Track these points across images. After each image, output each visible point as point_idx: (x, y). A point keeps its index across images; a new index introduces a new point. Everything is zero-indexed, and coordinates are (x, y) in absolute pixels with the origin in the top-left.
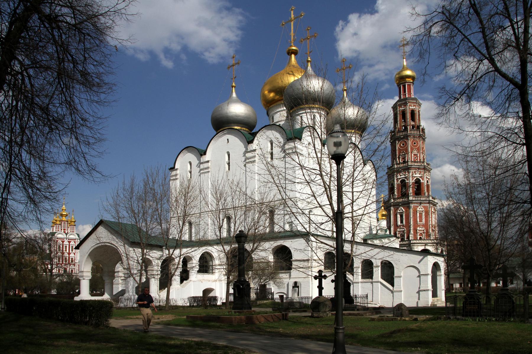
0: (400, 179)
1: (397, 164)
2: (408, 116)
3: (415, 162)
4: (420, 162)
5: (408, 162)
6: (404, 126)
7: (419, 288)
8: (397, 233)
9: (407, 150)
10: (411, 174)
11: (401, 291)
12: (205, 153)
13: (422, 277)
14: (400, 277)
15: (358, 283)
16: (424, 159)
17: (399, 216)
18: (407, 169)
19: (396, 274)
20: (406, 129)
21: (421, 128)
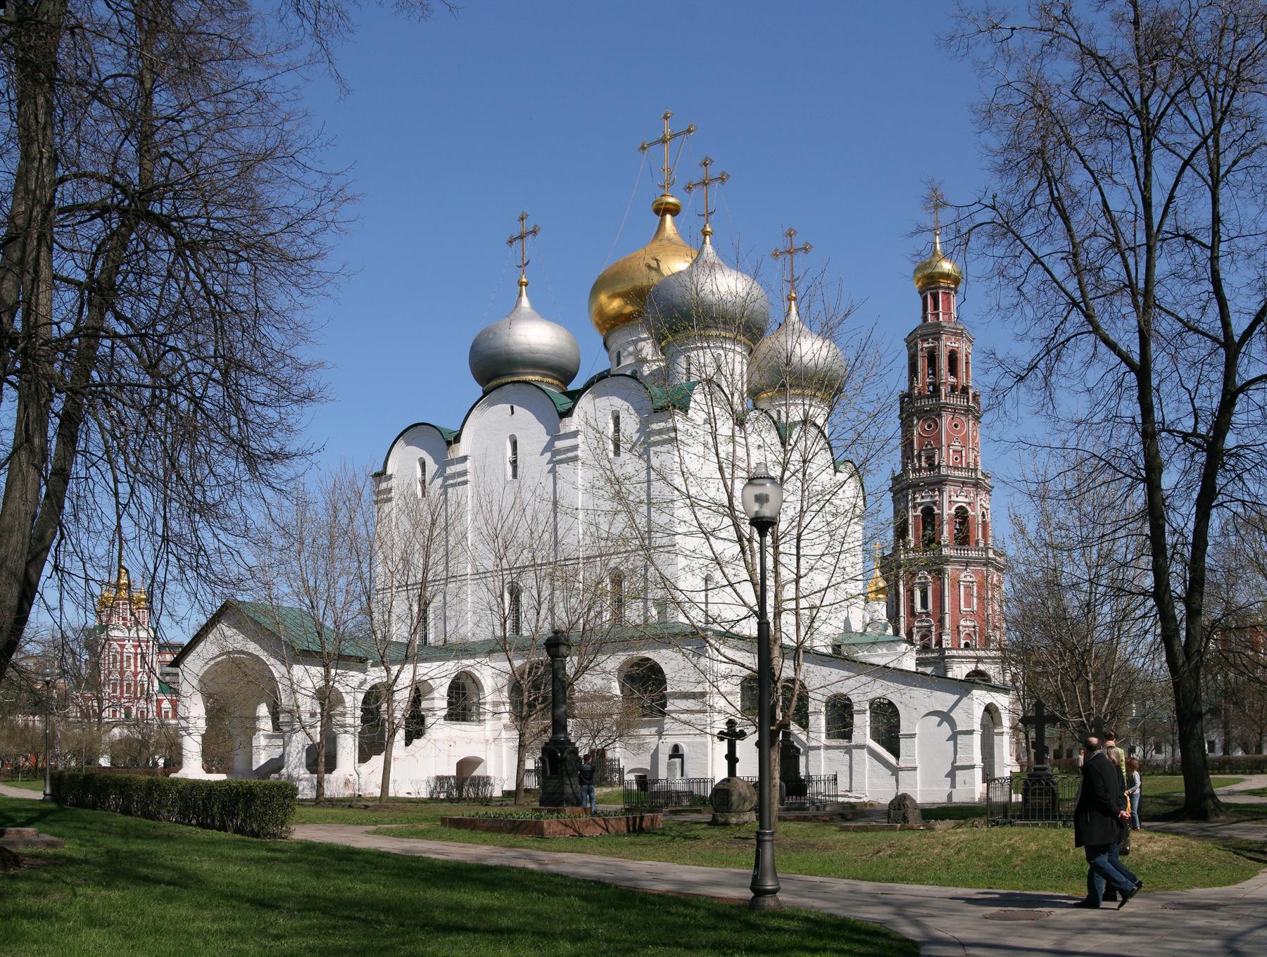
0: (920, 504)
1: (914, 471)
2: (944, 363)
3: (956, 468)
4: (968, 469)
5: (939, 466)
6: (930, 384)
7: (955, 761)
8: (915, 630)
9: (938, 439)
10: (946, 495)
11: (915, 769)
12: (457, 439)
13: (959, 737)
14: (912, 736)
15: (818, 748)
16: (976, 464)
17: (918, 594)
18: (938, 484)
19: (904, 729)
20: (936, 391)
21: (971, 392)
